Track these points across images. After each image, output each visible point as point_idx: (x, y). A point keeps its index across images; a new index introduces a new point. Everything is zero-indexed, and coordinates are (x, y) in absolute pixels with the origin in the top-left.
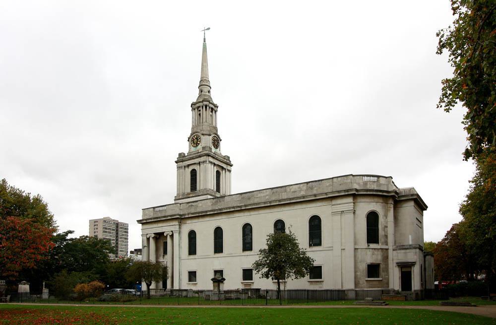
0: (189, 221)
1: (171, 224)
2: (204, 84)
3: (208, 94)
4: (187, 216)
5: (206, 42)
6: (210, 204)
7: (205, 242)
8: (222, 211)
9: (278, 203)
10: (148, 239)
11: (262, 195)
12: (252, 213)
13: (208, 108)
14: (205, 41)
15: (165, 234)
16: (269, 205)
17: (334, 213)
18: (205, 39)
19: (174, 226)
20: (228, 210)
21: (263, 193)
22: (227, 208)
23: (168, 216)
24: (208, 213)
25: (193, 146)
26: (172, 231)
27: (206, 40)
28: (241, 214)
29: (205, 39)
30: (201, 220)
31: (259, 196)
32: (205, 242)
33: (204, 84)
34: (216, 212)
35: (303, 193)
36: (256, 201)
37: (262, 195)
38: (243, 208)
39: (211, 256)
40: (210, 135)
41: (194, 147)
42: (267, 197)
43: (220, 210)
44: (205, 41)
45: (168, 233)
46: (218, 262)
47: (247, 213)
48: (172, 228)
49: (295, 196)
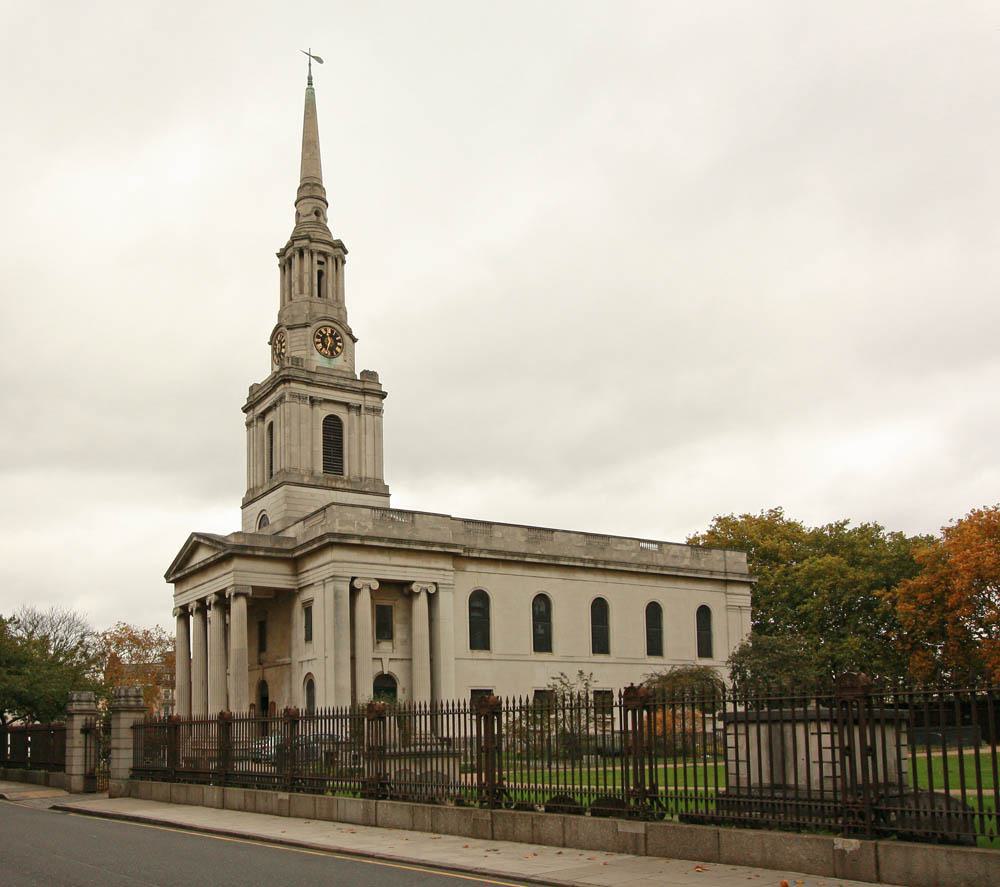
0: (471, 567)
1: (433, 564)
2: (311, 193)
3: (314, 217)
4: (475, 555)
5: (314, 86)
6: (523, 539)
7: (511, 623)
8: (557, 562)
9: (658, 572)
10: (354, 592)
11: (624, 547)
12: (611, 579)
13: (306, 255)
14: (310, 83)
15: (415, 588)
16: (644, 571)
17: (728, 608)
18: (310, 78)
19: (443, 572)
20: (571, 563)
21: (627, 545)
22: (570, 559)
23: (434, 544)
24: (528, 560)
25: (320, 351)
26: (435, 584)
27: (314, 81)
28: (589, 577)
29: (310, 78)
30: (502, 570)
31: (618, 548)
32: (511, 623)
33: (311, 193)
34: (544, 561)
35: (686, 563)
36: (615, 556)
37: (624, 547)
38: (600, 566)
39: (587, 659)
40: (306, 326)
41: (325, 355)
42: (634, 555)
43: (556, 558)
44: (310, 83)
45: (425, 586)
46: (541, 674)
47: (600, 578)
48: (437, 577)
49: (677, 565)
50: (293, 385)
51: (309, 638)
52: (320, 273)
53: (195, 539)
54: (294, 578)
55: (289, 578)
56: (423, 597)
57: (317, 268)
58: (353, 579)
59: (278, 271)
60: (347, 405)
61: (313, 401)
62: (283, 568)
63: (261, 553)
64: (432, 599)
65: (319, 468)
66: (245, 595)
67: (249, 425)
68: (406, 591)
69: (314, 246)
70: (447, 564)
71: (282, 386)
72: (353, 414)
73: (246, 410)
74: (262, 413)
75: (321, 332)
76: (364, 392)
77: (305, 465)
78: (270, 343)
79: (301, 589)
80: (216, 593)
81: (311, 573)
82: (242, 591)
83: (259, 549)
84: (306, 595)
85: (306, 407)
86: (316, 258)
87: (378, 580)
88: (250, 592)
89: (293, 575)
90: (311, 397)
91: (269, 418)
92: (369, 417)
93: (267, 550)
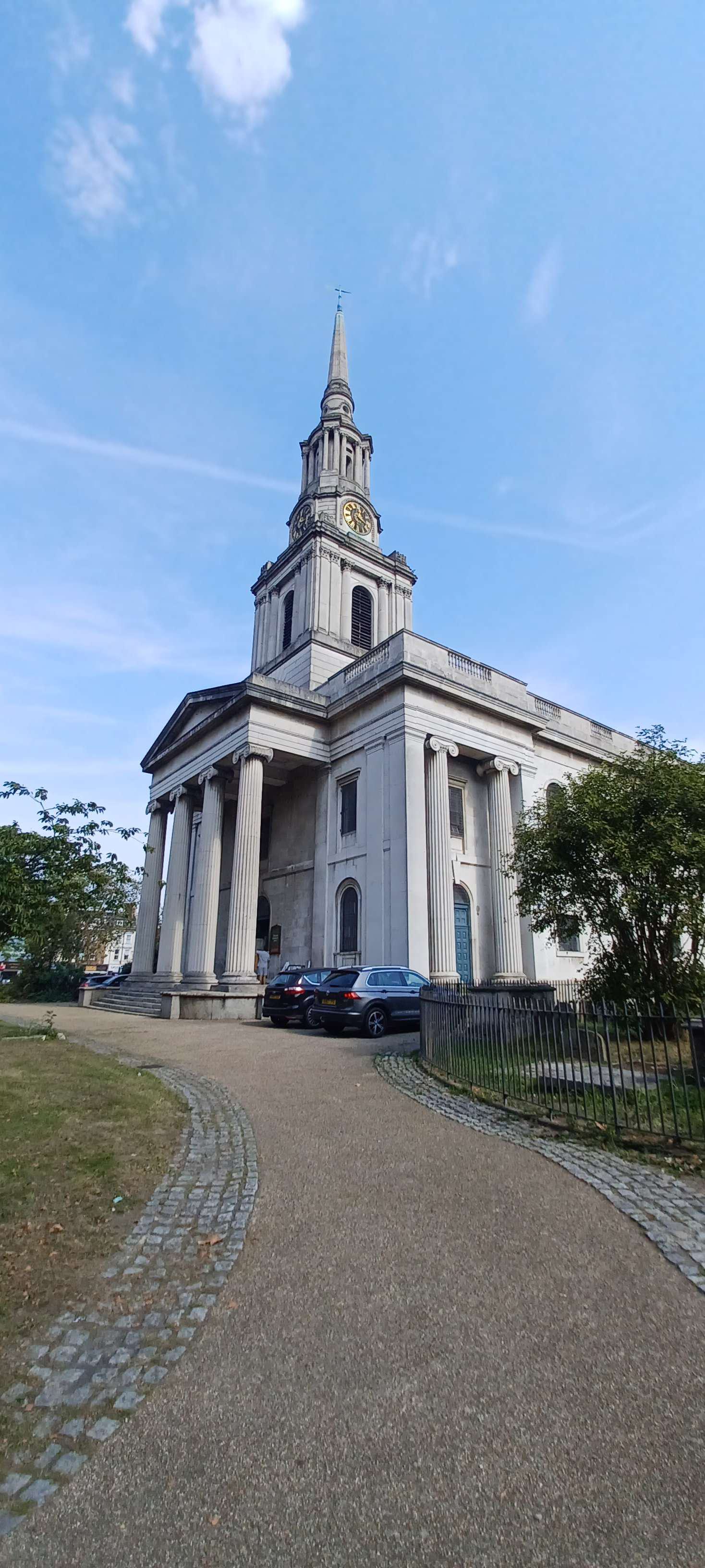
50: (323, 539)
51: (349, 825)
52: (348, 460)
53: (190, 701)
54: (327, 748)
55: (321, 746)
56: (505, 777)
57: (345, 453)
58: (429, 736)
59: (300, 462)
60: (378, 581)
61: (344, 564)
62: (309, 731)
63: (289, 705)
64: (515, 780)
65: (348, 635)
66: (262, 758)
67: (258, 604)
68: (480, 770)
69: (343, 430)
70: (526, 739)
71: (313, 540)
72: (384, 590)
73: (255, 590)
74: (277, 586)
75: (350, 505)
76: (396, 571)
77: (335, 628)
78: (289, 524)
79: (334, 763)
80: (215, 765)
81: (357, 734)
82: (259, 752)
83: (287, 697)
84: (345, 768)
85: (337, 567)
86: (344, 440)
87: (458, 744)
88: (270, 754)
89: (324, 743)
90: (342, 560)
91: (285, 591)
92: (400, 597)
93: (296, 701)
